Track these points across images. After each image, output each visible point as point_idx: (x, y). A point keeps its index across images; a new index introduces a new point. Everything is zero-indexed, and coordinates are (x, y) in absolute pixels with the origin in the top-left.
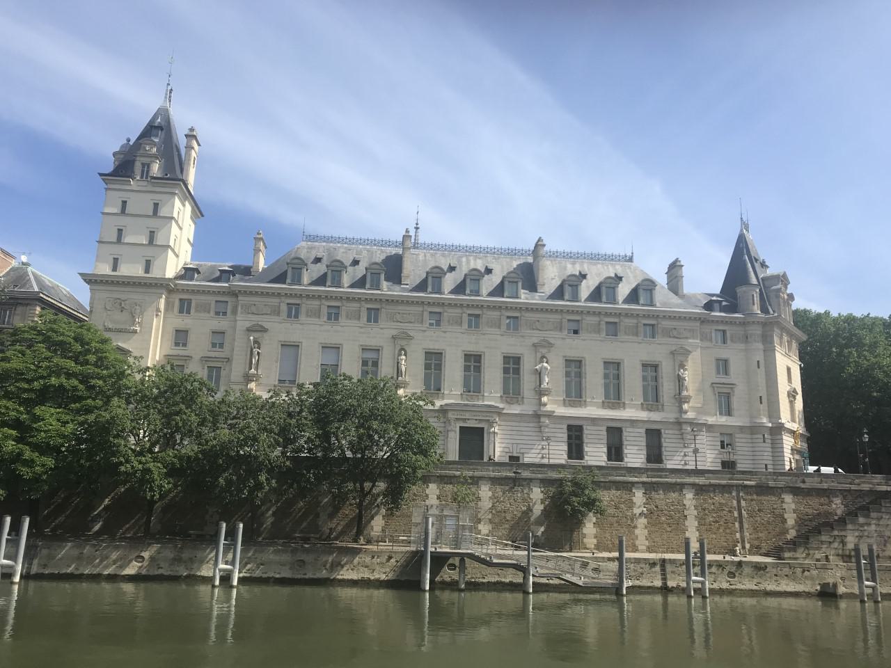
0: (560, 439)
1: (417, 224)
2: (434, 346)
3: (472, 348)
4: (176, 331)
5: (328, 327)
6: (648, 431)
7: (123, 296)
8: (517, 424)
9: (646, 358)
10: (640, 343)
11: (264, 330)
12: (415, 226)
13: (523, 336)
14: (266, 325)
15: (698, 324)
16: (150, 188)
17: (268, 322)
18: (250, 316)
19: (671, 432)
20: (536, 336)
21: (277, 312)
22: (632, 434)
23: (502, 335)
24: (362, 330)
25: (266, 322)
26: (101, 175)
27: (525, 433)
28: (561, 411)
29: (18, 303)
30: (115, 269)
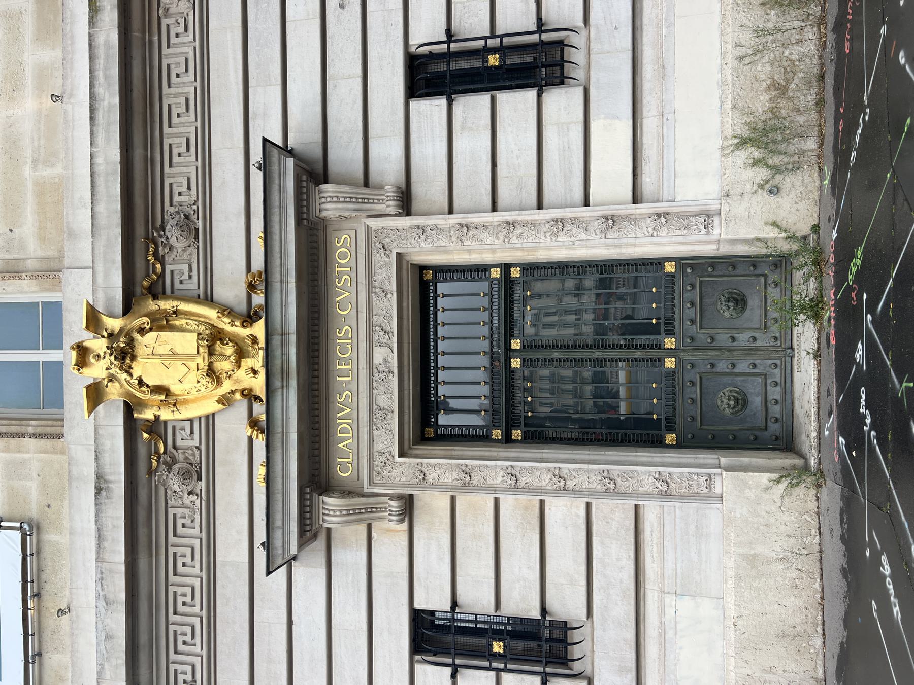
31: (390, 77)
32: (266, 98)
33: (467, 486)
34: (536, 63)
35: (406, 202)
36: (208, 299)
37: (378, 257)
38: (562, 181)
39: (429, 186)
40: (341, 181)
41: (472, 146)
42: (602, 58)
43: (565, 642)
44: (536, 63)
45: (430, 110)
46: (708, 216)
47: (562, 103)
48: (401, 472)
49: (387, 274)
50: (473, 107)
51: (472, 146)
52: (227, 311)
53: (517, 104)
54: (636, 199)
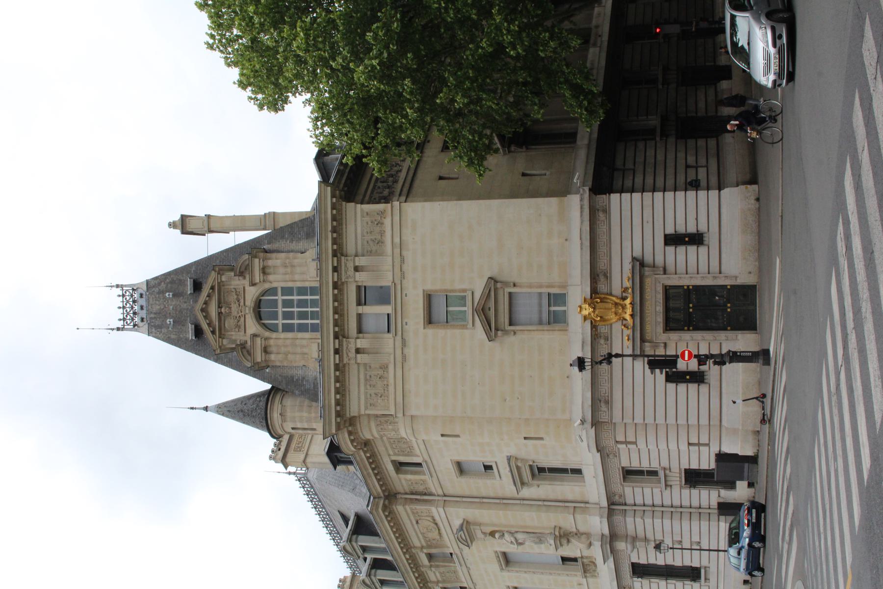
31: (660, 240)
32: (627, 244)
33: (680, 340)
34: (696, 239)
35: (665, 272)
36: (611, 294)
37: (658, 284)
38: (703, 268)
39: (671, 267)
40: (649, 266)
41: (681, 258)
42: (712, 239)
43: (703, 376)
44: (696, 239)
45: (670, 249)
46: (736, 277)
47: (703, 250)
48: (663, 337)
49: (660, 289)
50: (681, 249)
51: (681, 258)
52: (617, 297)
53: (692, 249)
54: (720, 273)
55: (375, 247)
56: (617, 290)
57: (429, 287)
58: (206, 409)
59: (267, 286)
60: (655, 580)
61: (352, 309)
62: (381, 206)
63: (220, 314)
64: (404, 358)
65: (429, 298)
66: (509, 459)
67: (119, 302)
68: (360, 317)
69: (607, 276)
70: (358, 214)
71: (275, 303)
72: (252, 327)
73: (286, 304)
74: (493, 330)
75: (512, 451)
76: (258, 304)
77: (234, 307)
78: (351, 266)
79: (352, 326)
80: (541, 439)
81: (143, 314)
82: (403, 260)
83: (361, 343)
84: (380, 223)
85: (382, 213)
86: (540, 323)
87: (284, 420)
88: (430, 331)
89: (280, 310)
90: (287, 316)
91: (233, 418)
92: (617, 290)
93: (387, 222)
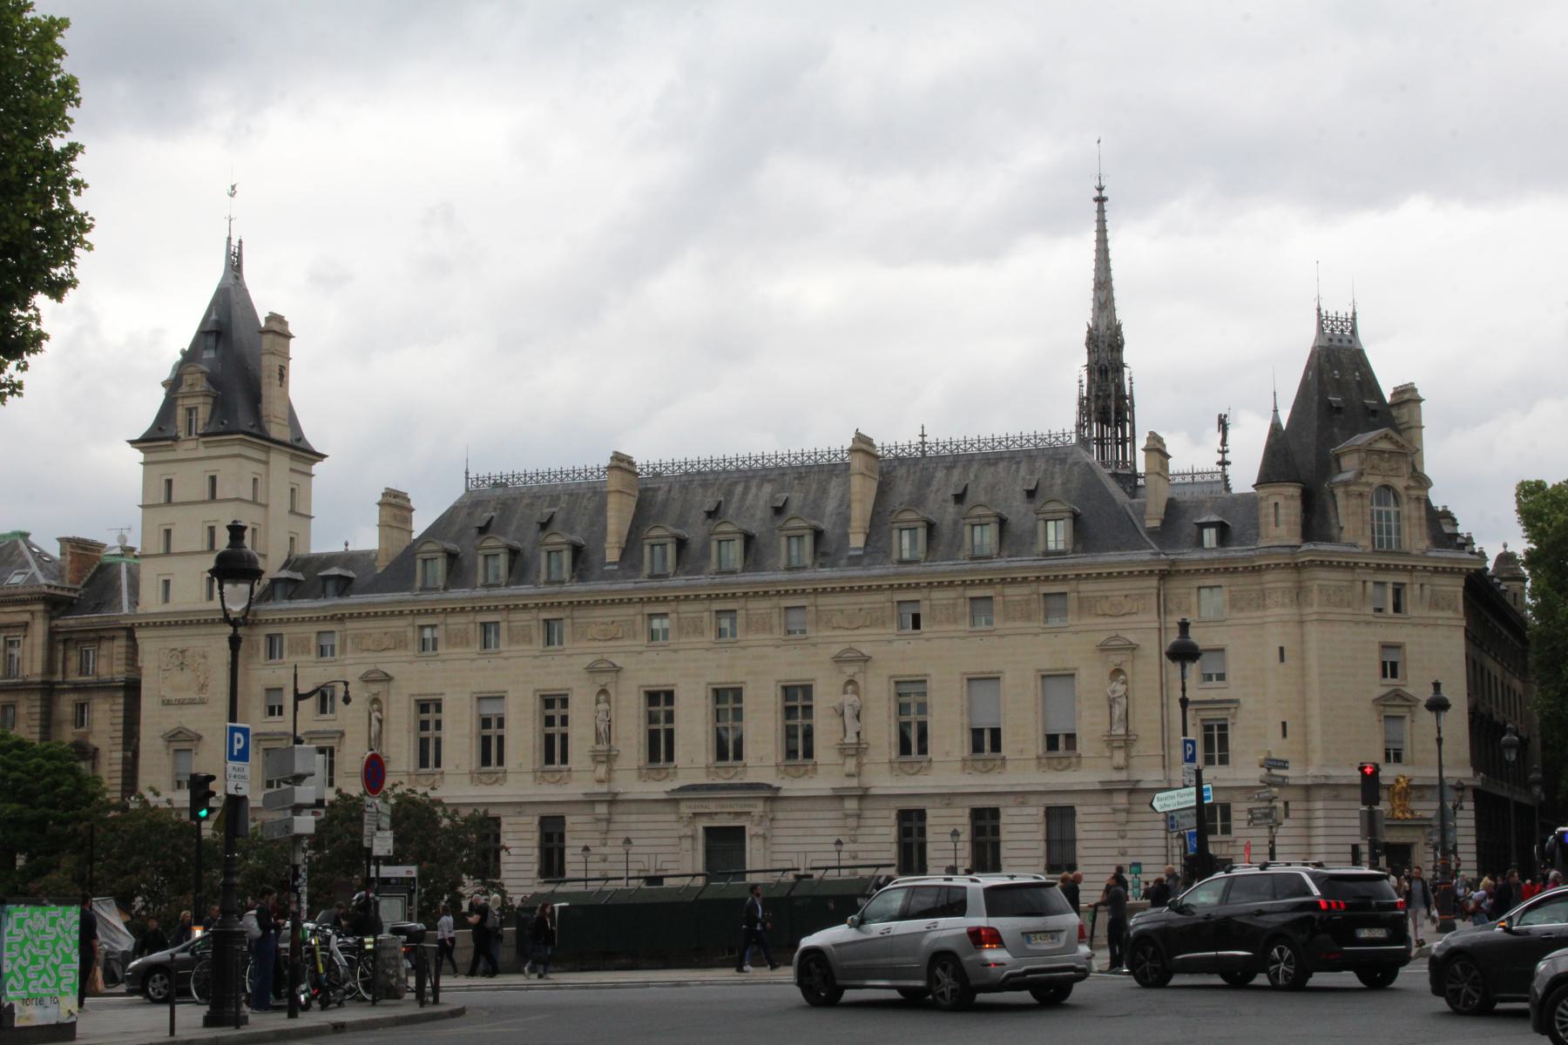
0: (883, 839)
1: (1100, 189)
2: (658, 681)
3: (723, 678)
4: (268, 690)
5: (483, 663)
6: (1050, 812)
7: (179, 644)
8: (806, 815)
9: (1047, 664)
10: (1037, 635)
11: (388, 678)
12: (1097, 194)
13: (814, 645)
14: (390, 669)
15: (1154, 582)
16: (203, 452)
17: (390, 663)
18: (365, 654)
19: (1093, 809)
20: (839, 640)
21: (400, 643)
22: (1017, 820)
23: (778, 647)
24: (538, 662)
25: (390, 663)
26: (132, 442)
27: (819, 831)
28: (883, 780)
29: (101, 638)
30: (166, 599)
55: (1435, 604)
56: (1414, 805)
57: (1408, 648)
58: (1276, 411)
59: (1405, 499)
60: (1043, 828)
61: (1391, 579)
62: (1461, 609)
63: (1382, 452)
64: (1357, 623)
65: (1397, 647)
66: (1236, 701)
67: (1341, 314)
68: (1383, 584)
69: (1421, 798)
70: (1454, 588)
71: (1387, 505)
72: (1377, 480)
73: (1388, 513)
74: (1381, 702)
75: (1248, 704)
76: (1387, 487)
77: (1385, 465)
78: (1425, 581)
79: (1380, 578)
80: (1285, 735)
81: (1335, 343)
82: (1426, 626)
83: (1370, 585)
84: (1449, 607)
85: (1456, 610)
86: (1386, 741)
87: (1286, 498)
88: (1377, 647)
89: (1384, 509)
90: (1380, 513)
91: (1270, 436)
92: (1414, 805)
93: (1450, 614)
